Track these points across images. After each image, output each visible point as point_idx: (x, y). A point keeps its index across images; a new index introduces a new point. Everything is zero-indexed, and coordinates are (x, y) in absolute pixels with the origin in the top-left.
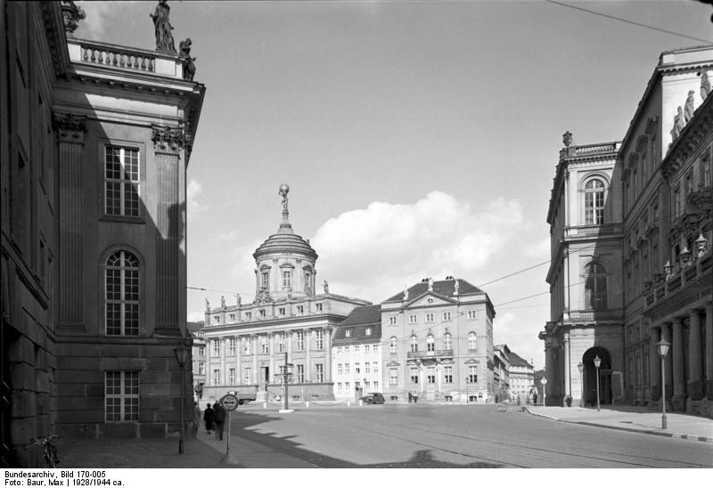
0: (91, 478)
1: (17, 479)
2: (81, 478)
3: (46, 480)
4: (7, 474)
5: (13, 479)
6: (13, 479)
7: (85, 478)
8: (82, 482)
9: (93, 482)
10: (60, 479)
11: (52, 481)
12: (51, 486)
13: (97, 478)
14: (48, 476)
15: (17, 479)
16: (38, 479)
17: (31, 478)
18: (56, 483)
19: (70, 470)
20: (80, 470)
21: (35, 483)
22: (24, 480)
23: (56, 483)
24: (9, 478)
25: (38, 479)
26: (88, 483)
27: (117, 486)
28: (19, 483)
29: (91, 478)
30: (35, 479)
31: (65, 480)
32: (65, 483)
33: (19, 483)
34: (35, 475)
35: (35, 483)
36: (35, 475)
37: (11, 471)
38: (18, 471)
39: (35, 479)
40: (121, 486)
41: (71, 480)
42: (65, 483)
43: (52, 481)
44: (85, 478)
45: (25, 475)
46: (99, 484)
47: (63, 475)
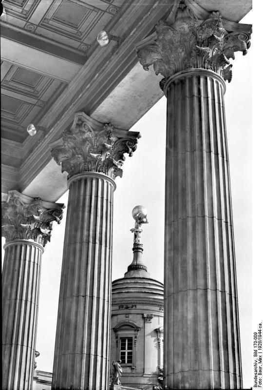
0: (257, 340)
1: (258, 381)
2: (258, 346)
3: (259, 365)
5: (258, 383)
6: (258, 383)
7: (258, 344)
8: (260, 345)
9: (260, 339)
10: (258, 357)
11: (259, 361)
13: (258, 337)
14: (256, 364)
15: (258, 381)
16: (258, 369)
17: (258, 373)
22: (259, 377)
24: (257, 385)
25: (258, 369)
26: (260, 342)
27: (262, 326)
29: (257, 340)
30: (258, 371)
31: (258, 355)
34: (256, 371)
36: (256, 371)
39: (258, 371)
40: (262, 324)
41: (258, 351)
43: (259, 361)
44: (258, 344)
46: (261, 336)
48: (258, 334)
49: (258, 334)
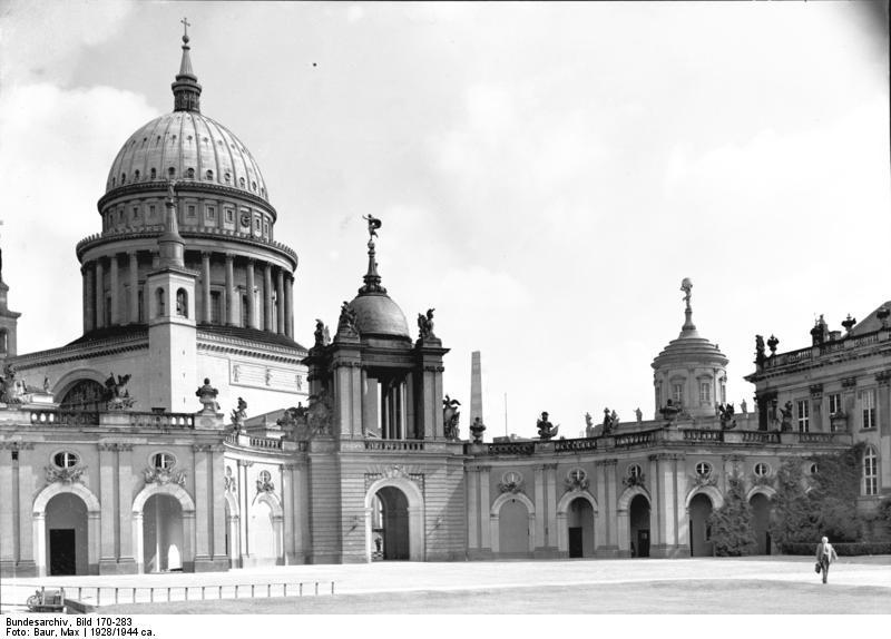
0: (113, 626)
1: (22, 628)
2: (101, 627)
3: (57, 629)
4: (9, 621)
5: (16, 628)
7: (106, 626)
8: (102, 632)
10: (74, 627)
11: (65, 630)
12: (64, 637)
13: (120, 628)
14: (60, 624)
15: (22, 628)
16: (47, 628)
17: (39, 627)
18: (70, 633)
21: (43, 633)
22: (30, 629)
23: (70, 633)
24: (12, 626)
25: (47, 628)
26: (109, 632)
27: (146, 637)
28: (24, 633)
32: (81, 633)
33: (24, 633)
34: (43, 623)
35: (43, 633)
36: (43, 623)
41: (89, 628)
42: (81, 633)
43: (65, 630)
44: (106, 626)
45: (31, 623)
47: (79, 622)
48: (127, 628)
49: (127, 628)
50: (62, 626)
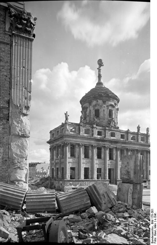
1: (154, 239)
4: (152, 243)
5: (154, 241)
10: (154, 225)
11: (155, 227)
15: (154, 239)
16: (154, 232)
18: (155, 226)
19: (151, 221)
20: (151, 217)
24: (153, 242)
25: (154, 232)
30: (154, 234)
34: (153, 233)
36: (153, 233)
37: (151, 241)
38: (151, 239)
41: (154, 221)
43: (155, 227)
45: (152, 236)
47: (152, 223)
50: (153, 228)
